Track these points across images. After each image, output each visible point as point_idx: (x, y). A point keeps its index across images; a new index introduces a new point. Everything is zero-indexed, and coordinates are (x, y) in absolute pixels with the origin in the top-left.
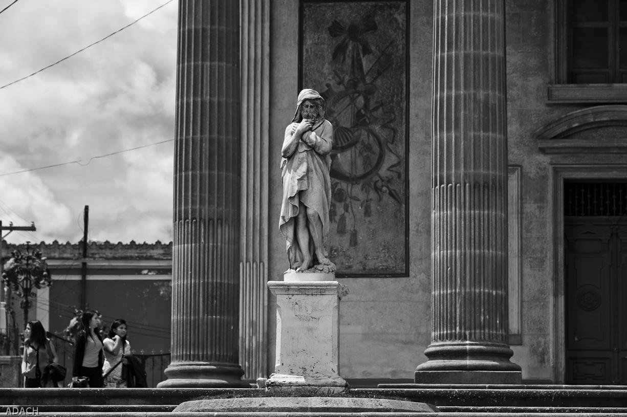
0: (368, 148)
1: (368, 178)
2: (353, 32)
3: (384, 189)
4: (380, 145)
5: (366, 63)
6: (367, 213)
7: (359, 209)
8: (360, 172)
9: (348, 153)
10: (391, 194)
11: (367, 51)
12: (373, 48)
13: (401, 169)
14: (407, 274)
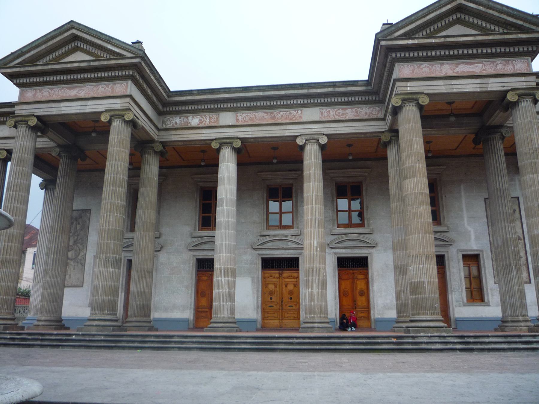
0: (76, 251)
1: (75, 259)
2: (76, 219)
4: (79, 250)
5: (78, 227)
6: (74, 269)
7: (72, 268)
8: (73, 258)
10: (81, 264)
11: (79, 224)
12: (80, 223)
13: (84, 257)
14: (82, 286)
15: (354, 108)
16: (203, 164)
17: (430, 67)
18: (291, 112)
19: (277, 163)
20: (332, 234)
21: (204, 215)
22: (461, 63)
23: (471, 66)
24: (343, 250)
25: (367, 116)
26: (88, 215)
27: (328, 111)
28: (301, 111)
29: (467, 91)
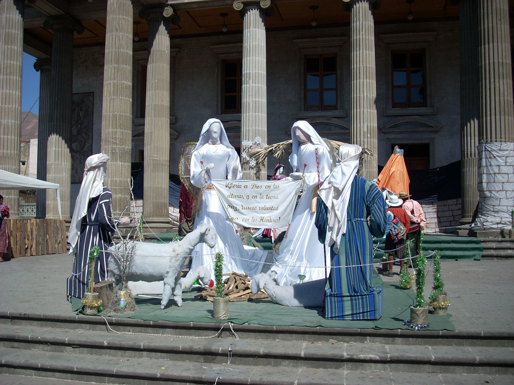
3: (86, 155)
4: (84, 140)
5: (81, 114)
9: (75, 143)
11: (81, 110)
12: (83, 109)
13: (91, 149)
16: (225, 30)
20: (386, 116)
21: (227, 94)
24: (400, 136)
26: (91, 99)
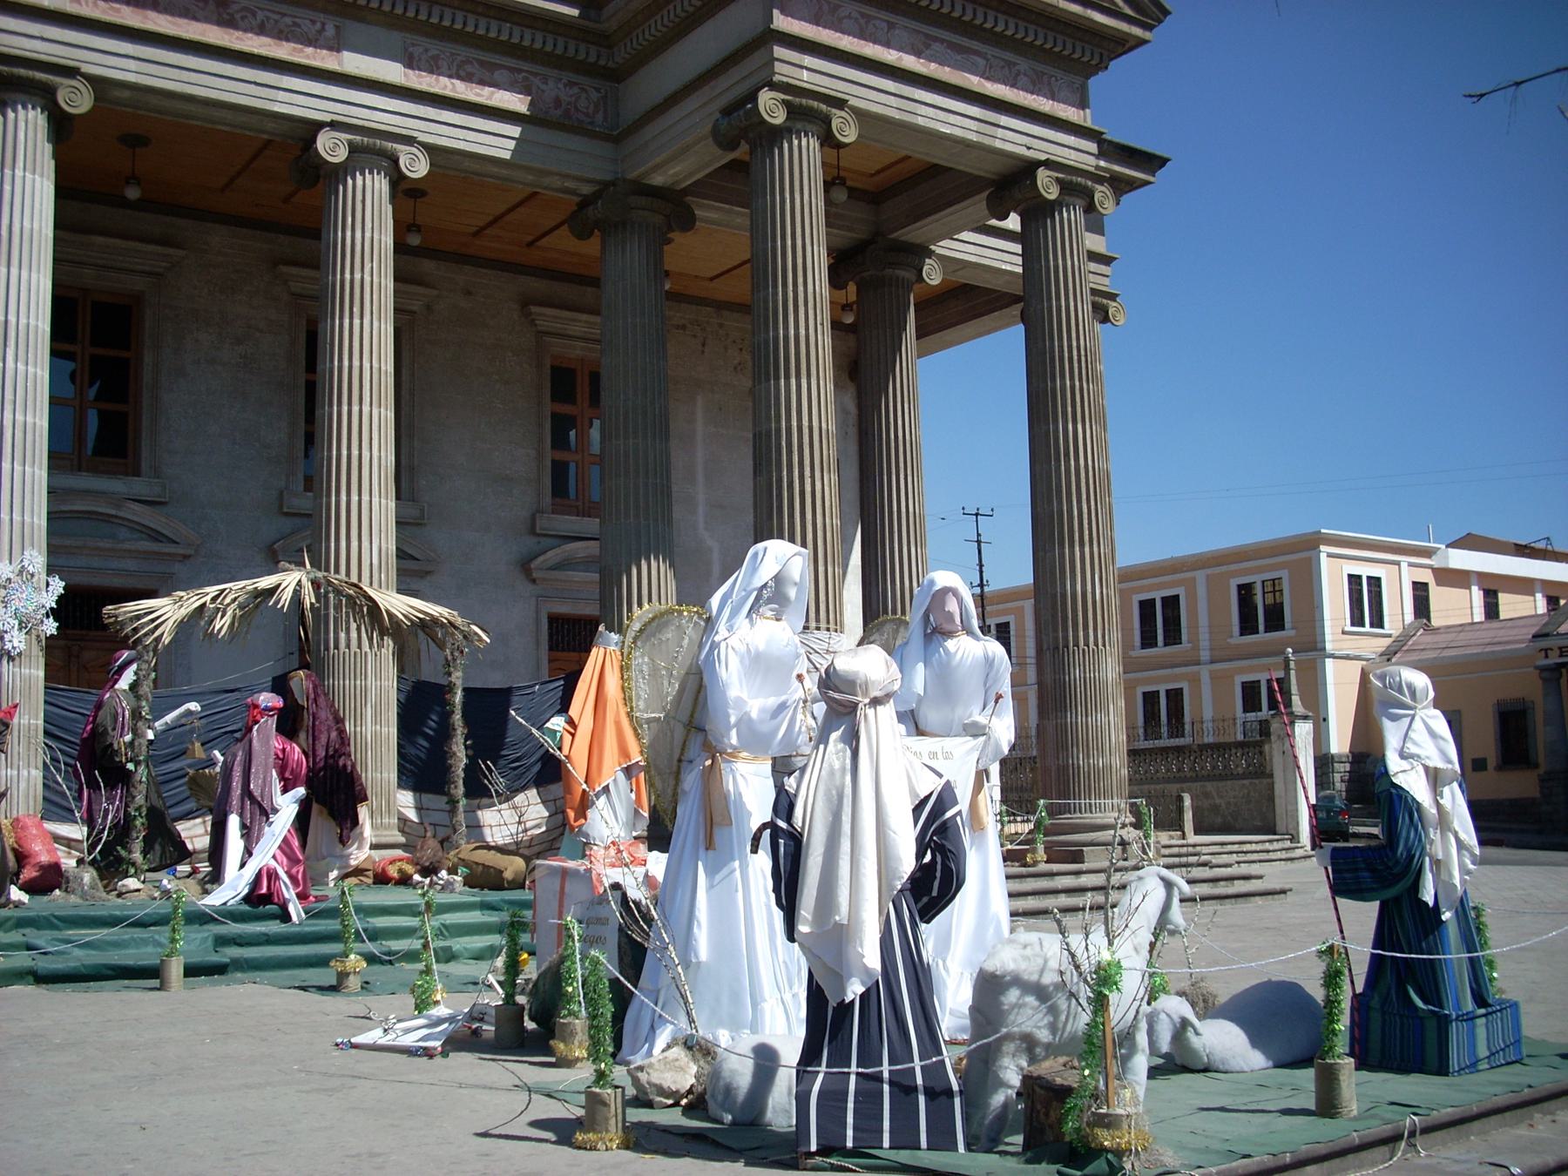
15: (520, 71)
17: (862, 21)
18: (297, 20)
19: (142, 205)
20: (287, 514)
22: (936, 39)
23: (959, 57)
25: (559, 112)
27: (433, 57)
28: (337, 27)
29: (948, 132)
